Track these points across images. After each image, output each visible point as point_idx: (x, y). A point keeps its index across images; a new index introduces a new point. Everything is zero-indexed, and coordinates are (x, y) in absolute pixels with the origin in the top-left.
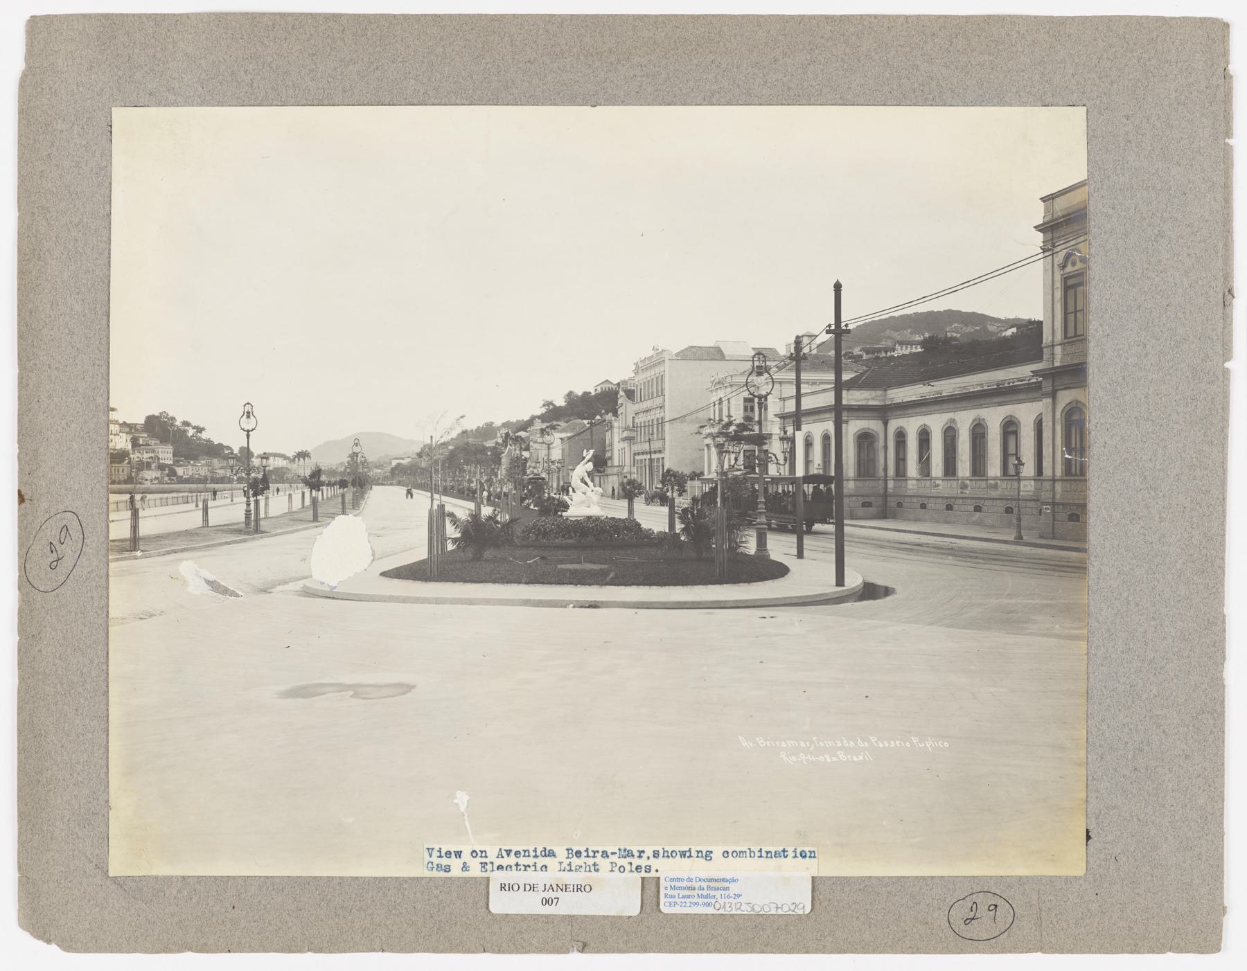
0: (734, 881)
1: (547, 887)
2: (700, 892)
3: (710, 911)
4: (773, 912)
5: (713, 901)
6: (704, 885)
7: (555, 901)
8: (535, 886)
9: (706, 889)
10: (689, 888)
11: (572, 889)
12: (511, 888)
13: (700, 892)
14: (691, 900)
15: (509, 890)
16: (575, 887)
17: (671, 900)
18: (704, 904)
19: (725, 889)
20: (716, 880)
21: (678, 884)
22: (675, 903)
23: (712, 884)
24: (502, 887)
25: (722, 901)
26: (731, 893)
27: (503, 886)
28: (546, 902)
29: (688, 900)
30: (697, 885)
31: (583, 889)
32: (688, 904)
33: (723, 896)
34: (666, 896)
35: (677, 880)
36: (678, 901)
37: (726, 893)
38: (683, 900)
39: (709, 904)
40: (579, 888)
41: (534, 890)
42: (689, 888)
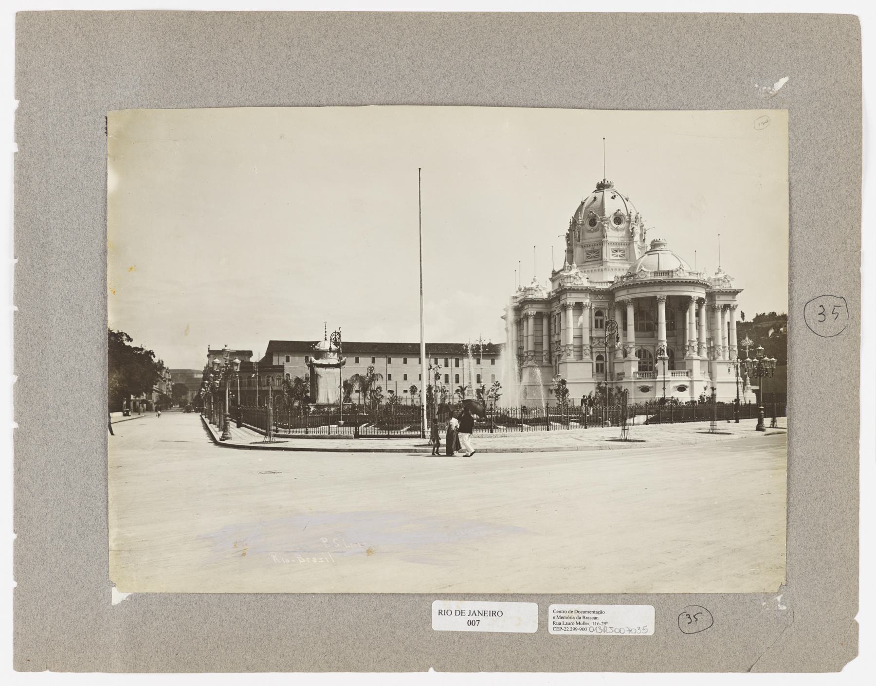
0: (601, 612)
1: (471, 614)
2: (578, 621)
3: (587, 633)
4: (627, 633)
5: (588, 626)
6: (581, 615)
7: (477, 623)
8: (463, 612)
9: (582, 618)
10: (570, 618)
11: (488, 614)
12: (446, 613)
13: (578, 621)
14: (573, 626)
15: (445, 615)
16: (491, 612)
18: (581, 629)
19: (595, 618)
20: (590, 612)
22: (561, 628)
23: (587, 615)
24: (440, 613)
25: (594, 626)
27: (440, 611)
28: (471, 623)
29: (569, 626)
30: (575, 615)
31: (496, 614)
32: (570, 629)
33: (594, 624)
34: (554, 623)
35: (563, 612)
36: (562, 626)
37: (597, 621)
38: (566, 626)
39: (584, 629)
40: (494, 613)
41: (462, 615)
42: (570, 618)
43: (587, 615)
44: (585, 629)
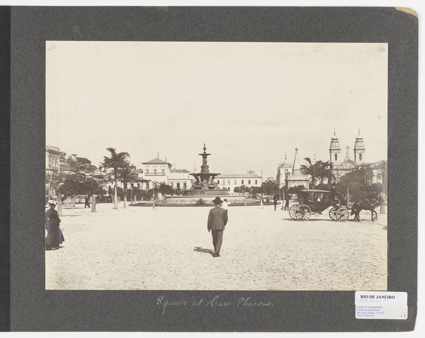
0: (381, 308)
2: (370, 311)
6: (371, 309)
17: (360, 314)
18: (371, 316)
19: (378, 310)
21: (362, 309)
22: (361, 315)
23: (373, 309)
26: (380, 312)
29: (365, 314)
30: (368, 309)
32: (365, 316)
34: (357, 313)
35: (362, 307)
36: (362, 314)
37: (379, 312)
38: (364, 314)
43: (373, 309)
44: (372, 316)
